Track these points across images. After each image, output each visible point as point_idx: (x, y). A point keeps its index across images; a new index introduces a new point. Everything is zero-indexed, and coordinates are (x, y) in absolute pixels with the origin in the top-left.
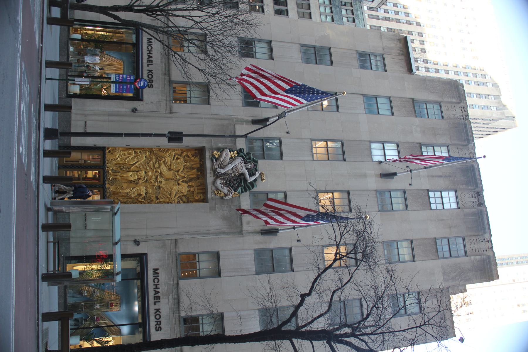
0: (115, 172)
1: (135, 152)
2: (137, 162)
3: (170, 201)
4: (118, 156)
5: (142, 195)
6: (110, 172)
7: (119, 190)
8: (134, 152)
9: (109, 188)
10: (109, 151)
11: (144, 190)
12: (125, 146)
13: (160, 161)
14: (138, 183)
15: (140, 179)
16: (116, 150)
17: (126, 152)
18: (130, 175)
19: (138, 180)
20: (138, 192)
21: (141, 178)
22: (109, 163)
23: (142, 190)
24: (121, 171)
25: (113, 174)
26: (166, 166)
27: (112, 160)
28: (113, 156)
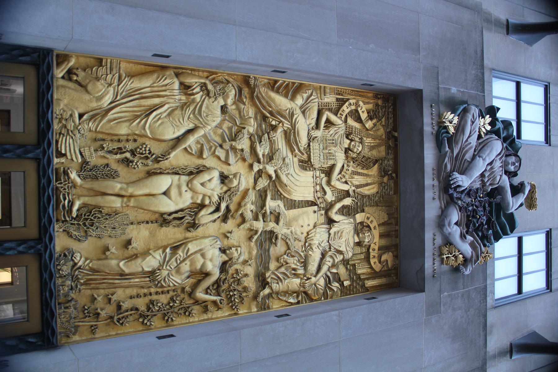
0: (96, 178)
1: (181, 84)
2: (190, 132)
3: (304, 287)
4: (108, 98)
5: (207, 275)
6: (73, 175)
7: (114, 262)
8: (176, 85)
9: (68, 254)
10: (70, 72)
11: (217, 252)
12: (147, 56)
13: (274, 128)
14: (193, 226)
15: (202, 206)
16: (101, 71)
17: (145, 83)
18: (164, 189)
19: (196, 214)
20: (192, 263)
21: (207, 202)
22: (66, 132)
23: (209, 255)
24: (122, 170)
25: (89, 184)
26: (292, 151)
27: (81, 116)
28: (87, 97)
